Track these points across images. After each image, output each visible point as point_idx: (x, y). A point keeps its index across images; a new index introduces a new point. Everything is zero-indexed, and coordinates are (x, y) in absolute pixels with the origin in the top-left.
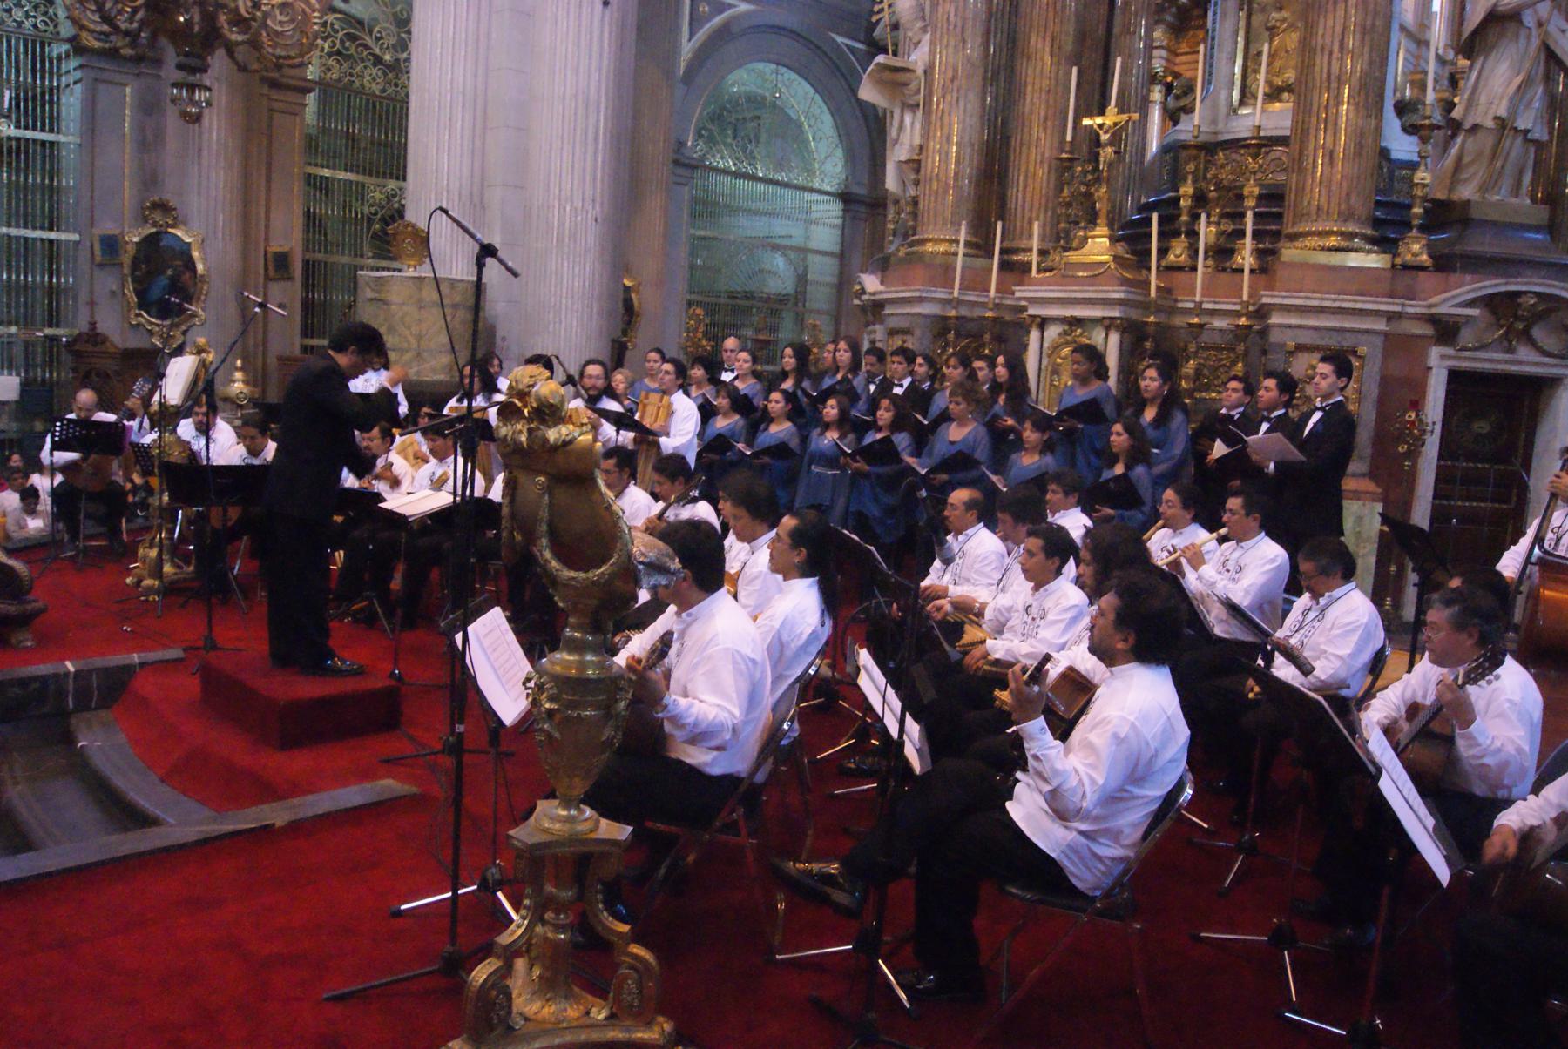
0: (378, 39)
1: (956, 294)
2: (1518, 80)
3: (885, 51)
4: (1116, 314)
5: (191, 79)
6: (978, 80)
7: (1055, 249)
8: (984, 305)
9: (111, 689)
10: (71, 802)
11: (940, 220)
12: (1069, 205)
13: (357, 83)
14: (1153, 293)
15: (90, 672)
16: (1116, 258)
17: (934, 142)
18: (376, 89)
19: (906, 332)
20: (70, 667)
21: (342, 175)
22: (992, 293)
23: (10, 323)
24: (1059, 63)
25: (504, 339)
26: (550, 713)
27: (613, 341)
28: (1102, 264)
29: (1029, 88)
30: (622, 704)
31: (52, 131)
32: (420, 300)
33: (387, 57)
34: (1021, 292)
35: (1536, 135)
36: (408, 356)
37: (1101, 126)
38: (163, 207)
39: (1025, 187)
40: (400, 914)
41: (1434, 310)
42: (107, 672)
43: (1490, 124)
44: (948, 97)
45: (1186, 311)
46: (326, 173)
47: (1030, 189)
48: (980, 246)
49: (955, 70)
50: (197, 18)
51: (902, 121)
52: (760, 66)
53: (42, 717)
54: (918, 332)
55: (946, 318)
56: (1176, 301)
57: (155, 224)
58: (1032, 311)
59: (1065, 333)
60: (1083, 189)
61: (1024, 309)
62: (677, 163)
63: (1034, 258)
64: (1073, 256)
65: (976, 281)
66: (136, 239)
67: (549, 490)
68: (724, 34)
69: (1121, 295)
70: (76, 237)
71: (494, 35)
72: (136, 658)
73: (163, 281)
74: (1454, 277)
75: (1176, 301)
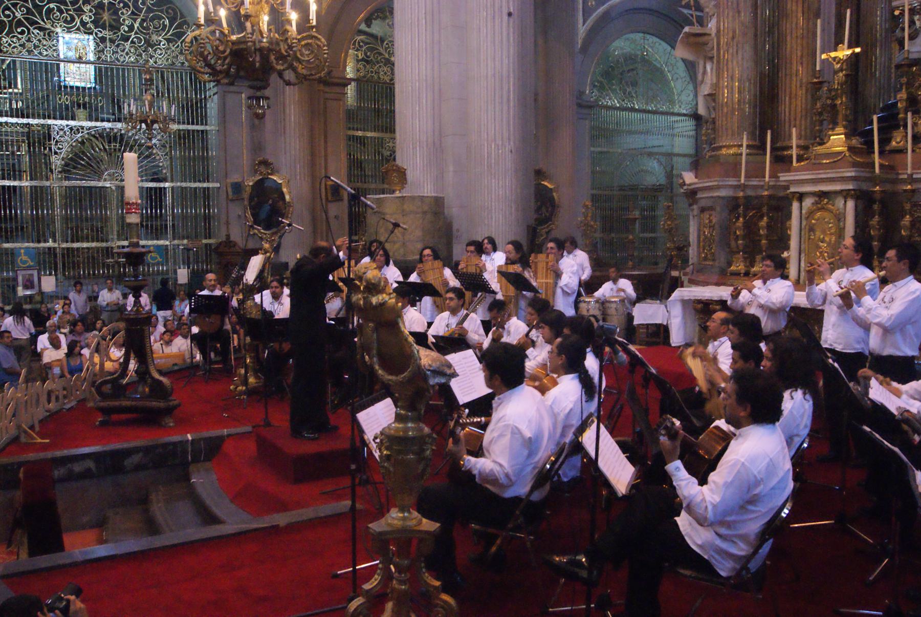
0: (386, 49)
3: (691, 24)
4: (851, 187)
5: (259, 94)
6: (751, 34)
7: (813, 144)
8: (762, 187)
9: (211, 450)
10: (185, 509)
11: (730, 132)
12: (820, 114)
13: (376, 77)
14: (877, 170)
15: (201, 439)
16: (851, 149)
17: (730, 80)
19: (711, 208)
20: (189, 437)
21: (369, 134)
22: (767, 179)
23: (183, 238)
24: (809, 19)
25: (458, 230)
26: (388, 457)
27: (528, 226)
28: (840, 153)
29: (789, 38)
30: (428, 452)
31: (202, 124)
32: (403, 211)
34: (784, 177)
36: (397, 246)
37: (834, 59)
38: (265, 163)
39: (790, 103)
40: (337, 576)
42: (206, 440)
44: (731, 51)
45: (904, 181)
46: (360, 133)
47: (793, 106)
48: (758, 148)
49: (734, 32)
50: (258, 59)
51: (705, 67)
52: (632, 36)
53: (173, 464)
54: (718, 209)
55: (736, 199)
56: (898, 174)
57: (261, 173)
58: (792, 189)
59: (816, 203)
60: (829, 102)
61: (787, 187)
62: (580, 106)
63: (794, 152)
64: (820, 149)
65: (756, 171)
66: (251, 184)
67: (376, 329)
68: (606, 17)
69: (853, 174)
70: (218, 185)
72: (225, 432)
73: (266, 208)
75: (898, 174)
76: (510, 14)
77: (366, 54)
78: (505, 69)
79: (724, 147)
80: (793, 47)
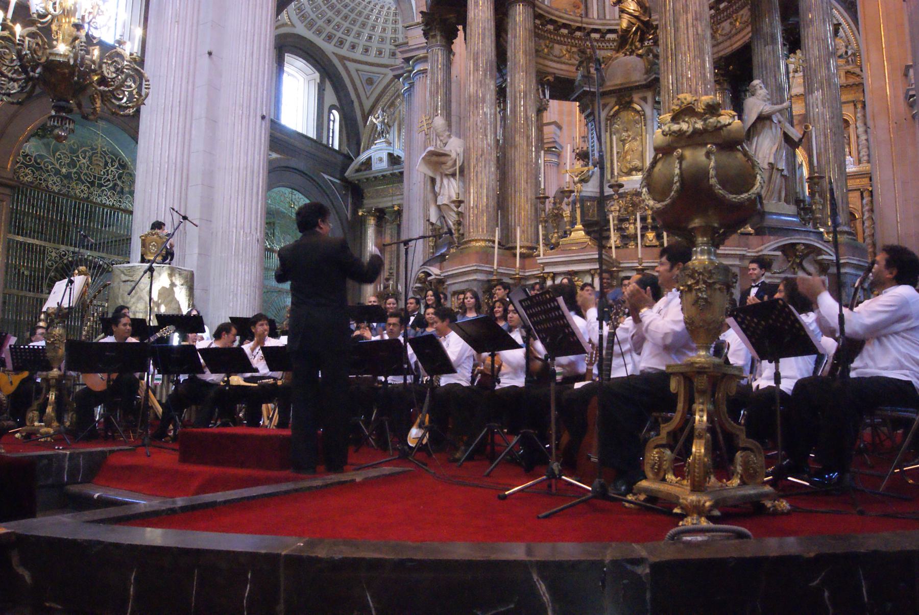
0: (58, 159)
1: (495, 267)
2: (776, 146)
18: (56, 189)
33: (64, 170)
35: (785, 173)
41: (760, 253)
43: (766, 166)
49: (483, 151)
52: (283, 189)
58: (547, 270)
71: (193, 132)
74: (766, 238)
76: (263, 117)
77: (36, 161)
78: (256, 167)
79: (473, 240)
80: (520, 171)
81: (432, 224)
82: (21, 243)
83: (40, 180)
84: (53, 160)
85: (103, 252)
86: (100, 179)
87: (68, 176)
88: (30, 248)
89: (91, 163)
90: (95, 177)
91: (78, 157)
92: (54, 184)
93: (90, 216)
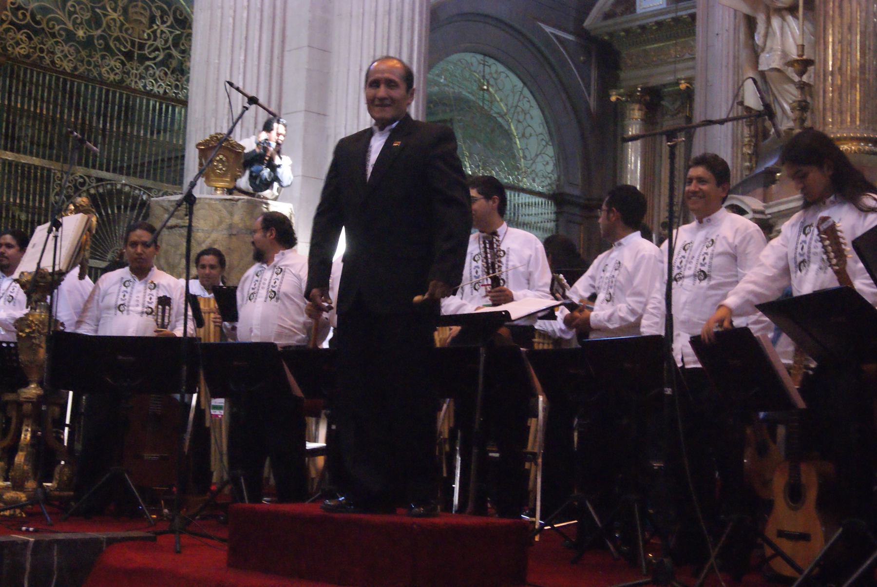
0: (70, 14)
18: (68, 67)
33: (81, 33)
81: (748, 109)
82: (10, 163)
83: (42, 51)
84: (60, 15)
85: (148, 178)
86: (141, 47)
87: (88, 43)
88: (27, 172)
89: (126, 19)
90: (133, 43)
91: (104, 8)
92: (65, 57)
93: (128, 113)
